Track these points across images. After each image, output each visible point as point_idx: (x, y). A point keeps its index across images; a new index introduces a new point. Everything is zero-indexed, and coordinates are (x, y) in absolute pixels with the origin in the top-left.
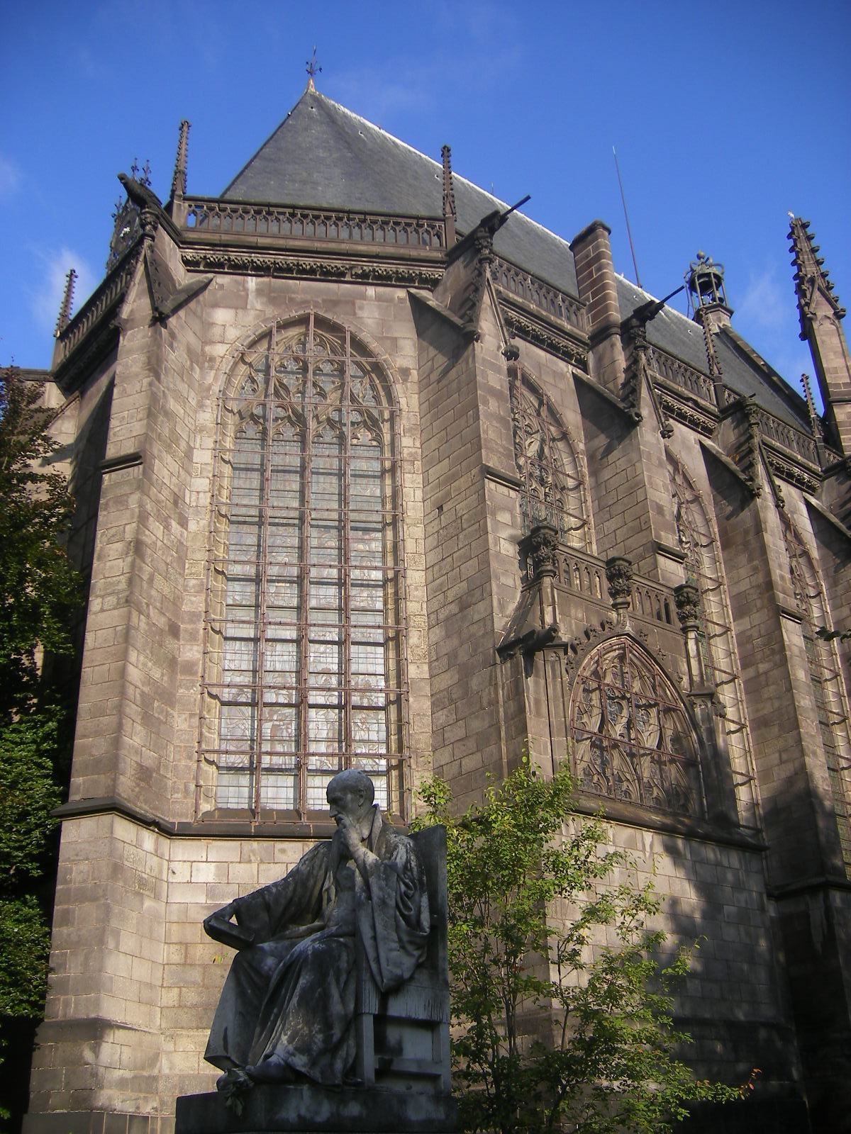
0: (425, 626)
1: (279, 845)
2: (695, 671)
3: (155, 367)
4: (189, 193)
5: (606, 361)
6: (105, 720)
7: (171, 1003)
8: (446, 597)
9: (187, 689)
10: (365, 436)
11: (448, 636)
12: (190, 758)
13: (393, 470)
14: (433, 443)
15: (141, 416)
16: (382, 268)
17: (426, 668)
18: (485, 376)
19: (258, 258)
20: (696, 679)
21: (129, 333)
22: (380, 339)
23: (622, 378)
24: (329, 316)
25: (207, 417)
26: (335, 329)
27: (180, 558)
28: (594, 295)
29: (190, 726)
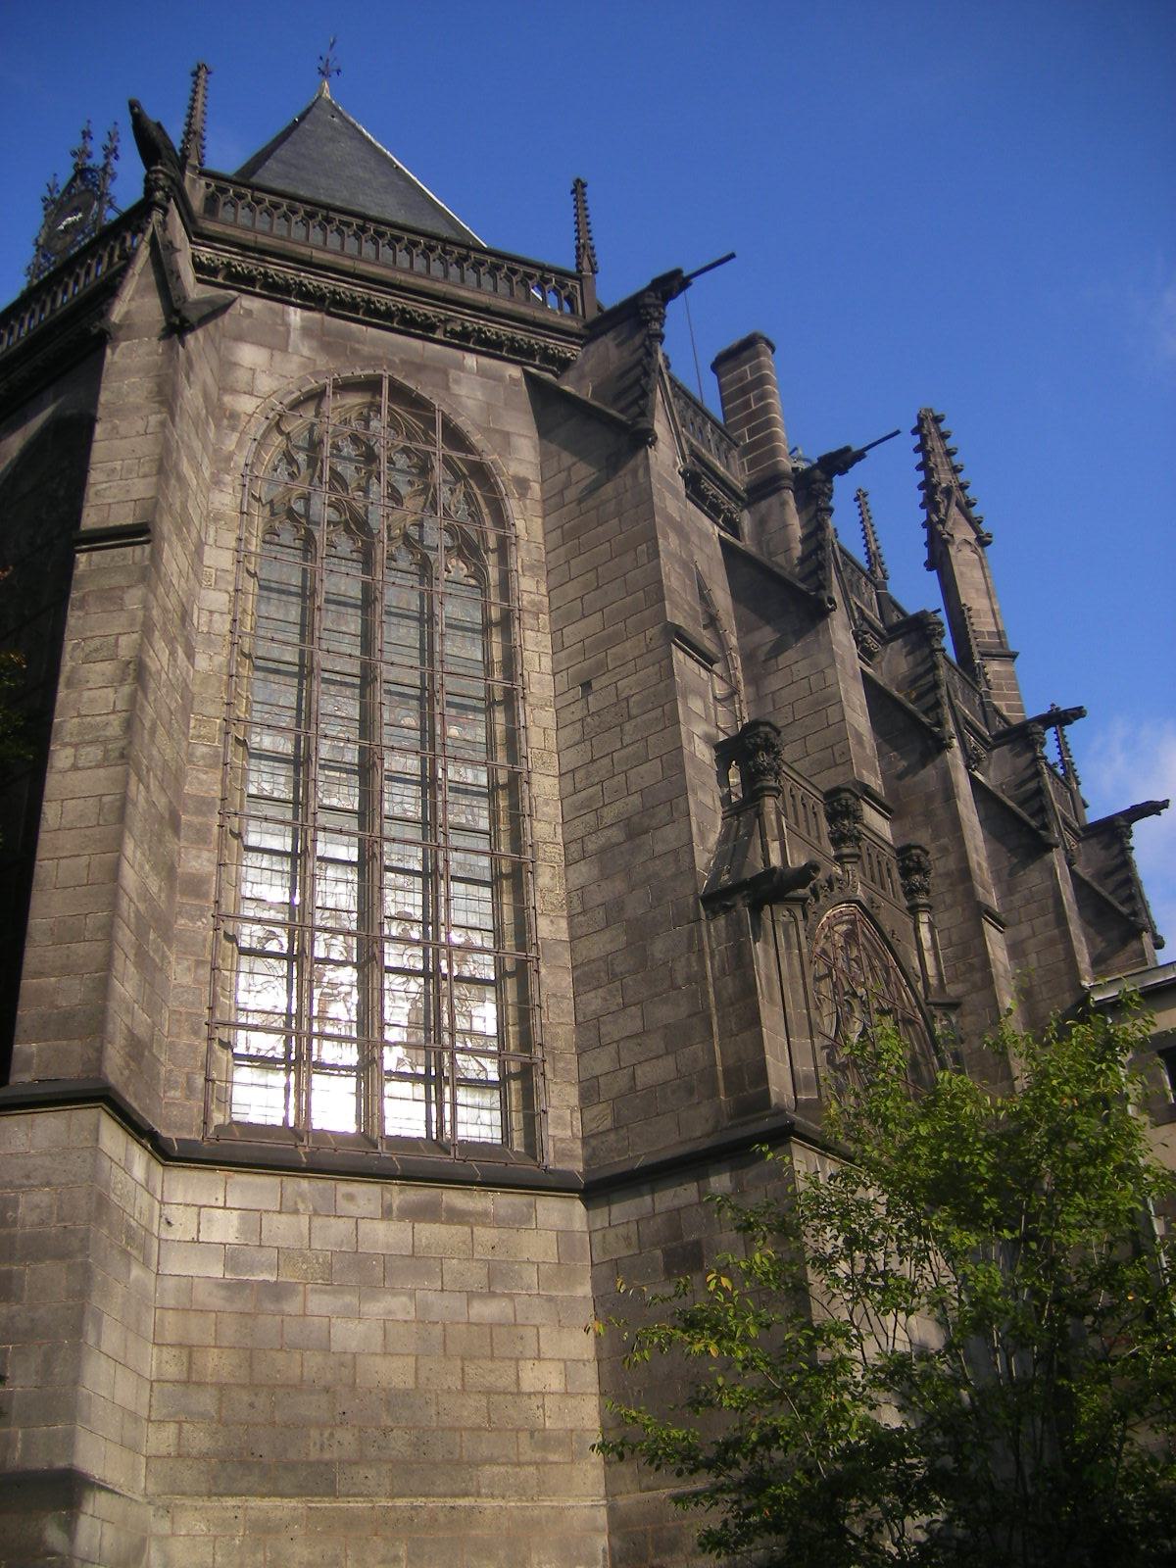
0: (560, 859)
1: (344, 1188)
2: (931, 971)
3: (166, 397)
4: (208, 166)
5: (773, 525)
6: (81, 948)
7: (163, 1450)
8: (600, 818)
9: (192, 919)
10: (459, 569)
11: (605, 876)
12: (196, 1033)
13: (506, 622)
14: (573, 590)
15: (145, 469)
16: (493, 329)
17: (564, 924)
18: (663, 499)
19: (310, 280)
20: (933, 981)
21: (123, 344)
22: (487, 431)
23: (797, 550)
24: (411, 384)
25: (226, 500)
26: (418, 405)
27: (184, 707)
28: (752, 432)
29: (196, 980)
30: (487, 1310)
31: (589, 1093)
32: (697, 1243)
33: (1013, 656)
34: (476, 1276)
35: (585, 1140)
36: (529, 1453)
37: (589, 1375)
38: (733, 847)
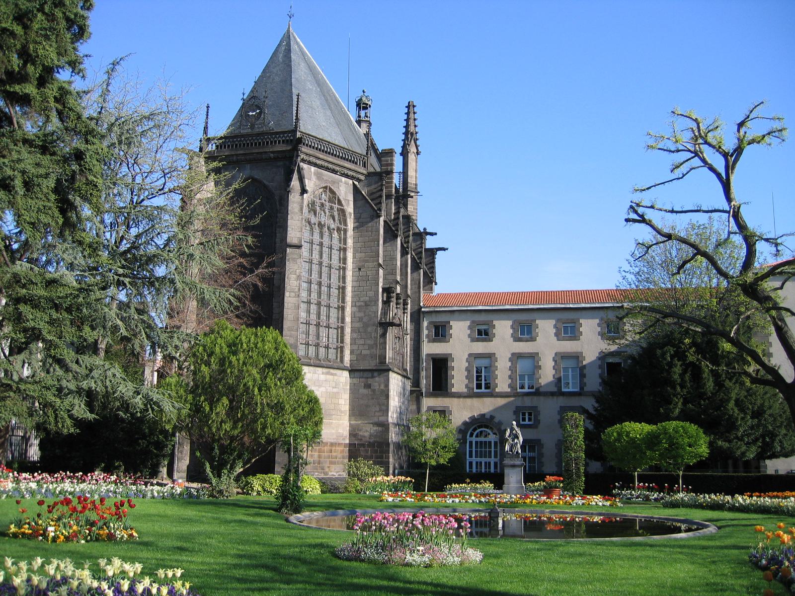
14: (359, 245)
19: (318, 162)
31: (352, 352)
32: (370, 384)
33: (418, 192)
34: (334, 385)
35: (350, 361)
36: (339, 414)
37: (348, 401)
38: (385, 313)
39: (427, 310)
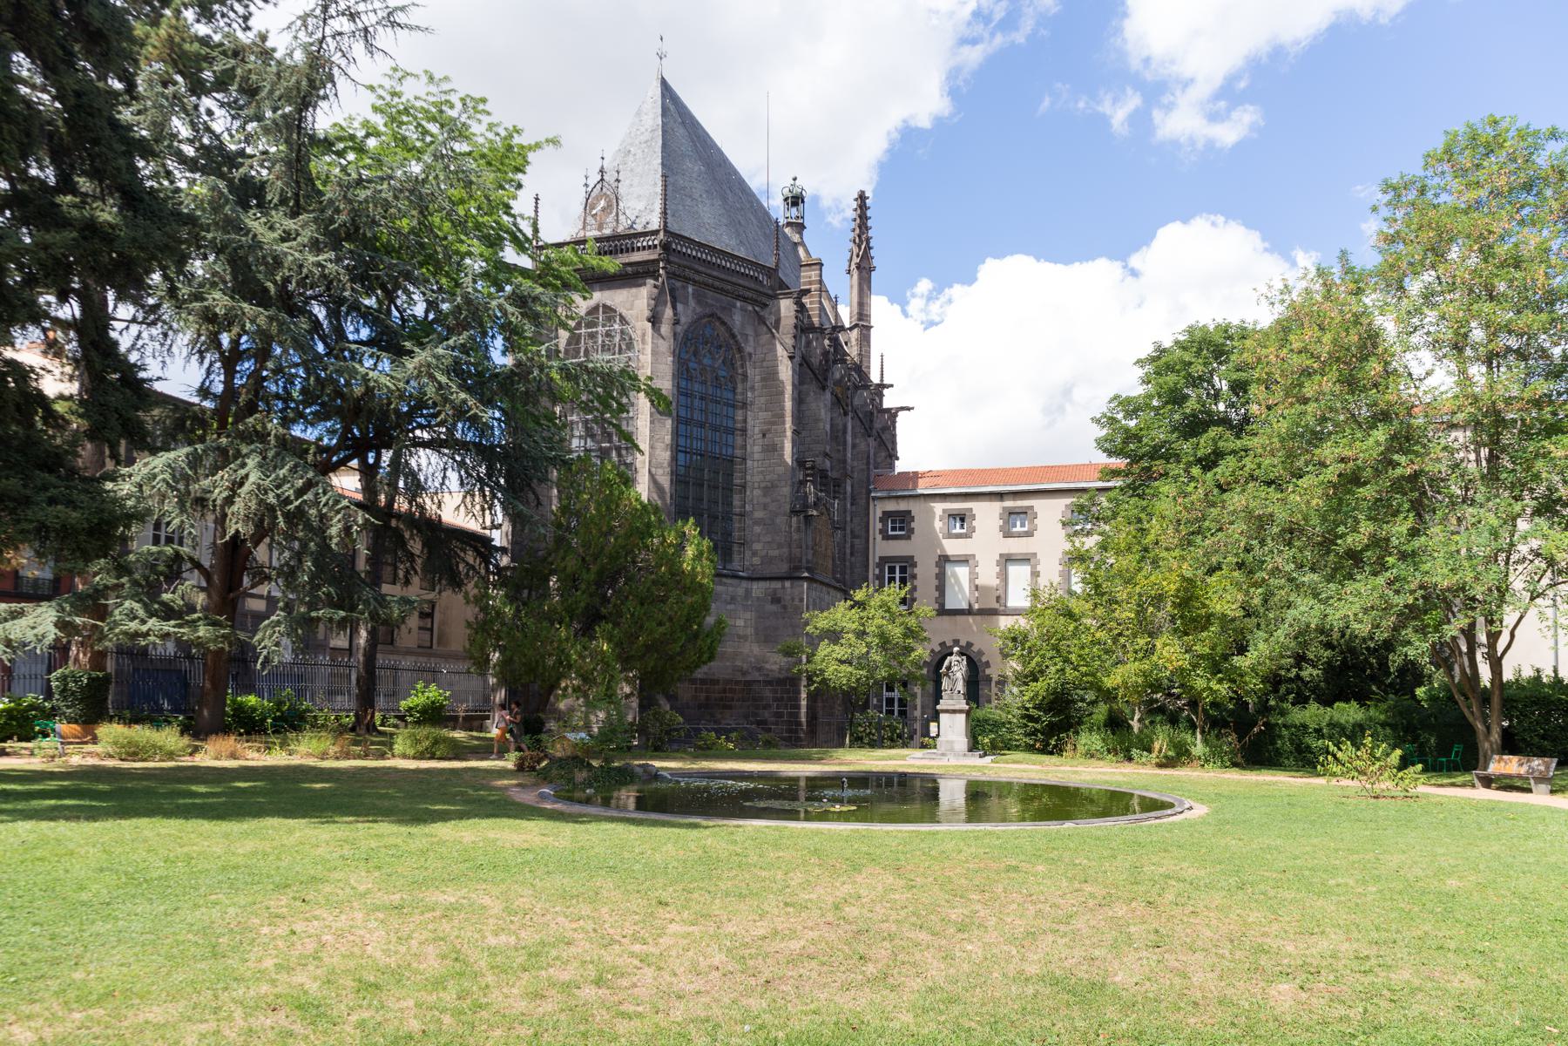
16: (749, 294)
19: (697, 277)
22: (742, 334)
30: (729, 607)
39: (879, 494)
